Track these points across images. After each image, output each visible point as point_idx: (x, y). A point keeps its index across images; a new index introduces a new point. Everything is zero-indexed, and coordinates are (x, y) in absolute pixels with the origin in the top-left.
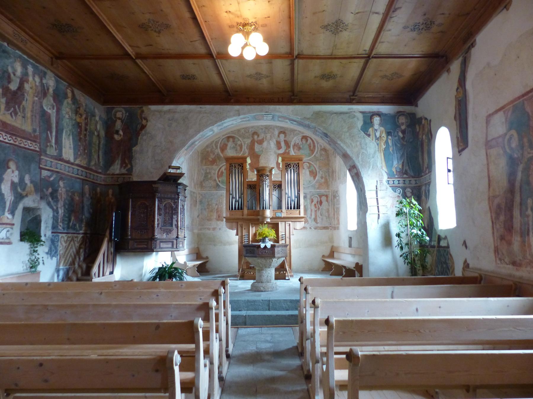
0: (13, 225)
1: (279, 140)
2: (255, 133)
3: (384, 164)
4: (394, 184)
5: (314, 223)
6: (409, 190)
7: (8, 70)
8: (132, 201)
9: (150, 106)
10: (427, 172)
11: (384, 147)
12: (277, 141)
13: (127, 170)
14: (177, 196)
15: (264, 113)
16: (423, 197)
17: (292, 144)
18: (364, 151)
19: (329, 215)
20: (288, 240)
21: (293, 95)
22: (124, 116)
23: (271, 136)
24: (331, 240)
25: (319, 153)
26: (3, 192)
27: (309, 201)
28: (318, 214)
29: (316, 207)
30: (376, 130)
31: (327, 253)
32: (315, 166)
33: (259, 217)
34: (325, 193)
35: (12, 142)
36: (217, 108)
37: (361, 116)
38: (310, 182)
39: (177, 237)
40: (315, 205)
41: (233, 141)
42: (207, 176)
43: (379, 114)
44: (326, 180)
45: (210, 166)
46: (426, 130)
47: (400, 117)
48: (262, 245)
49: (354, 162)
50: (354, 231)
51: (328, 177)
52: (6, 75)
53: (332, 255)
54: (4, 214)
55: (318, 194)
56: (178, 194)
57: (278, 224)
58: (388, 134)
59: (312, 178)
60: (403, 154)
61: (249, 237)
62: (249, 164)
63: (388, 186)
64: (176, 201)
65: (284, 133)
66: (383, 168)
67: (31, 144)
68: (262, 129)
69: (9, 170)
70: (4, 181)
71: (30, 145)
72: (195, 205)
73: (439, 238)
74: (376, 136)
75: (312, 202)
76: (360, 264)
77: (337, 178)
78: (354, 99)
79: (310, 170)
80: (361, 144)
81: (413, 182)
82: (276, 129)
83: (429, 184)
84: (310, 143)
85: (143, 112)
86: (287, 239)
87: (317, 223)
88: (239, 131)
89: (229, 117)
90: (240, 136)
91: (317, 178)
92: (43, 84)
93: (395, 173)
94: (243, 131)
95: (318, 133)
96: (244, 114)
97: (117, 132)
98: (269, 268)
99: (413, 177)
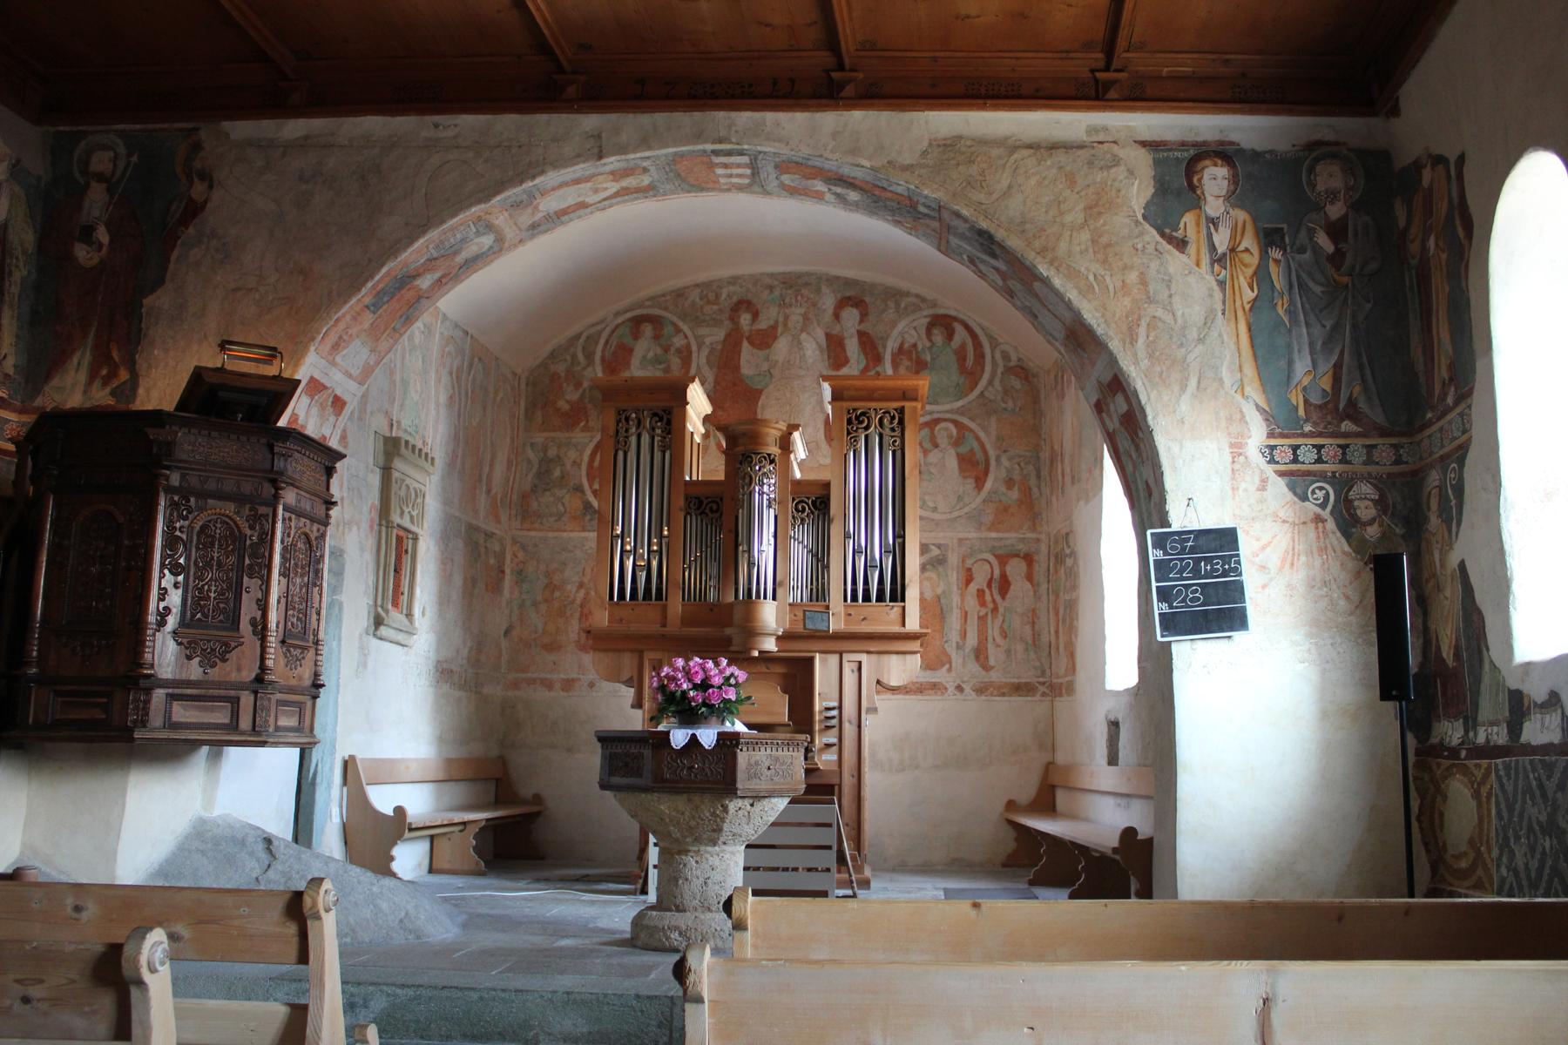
1: (836, 330)
2: (744, 304)
3: (1250, 370)
4: (1295, 460)
5: (973, 667)
6: (1363, 492)
8: (57, 506)
9: (226, 125)
10: (1450, 400)
11: (1249, 295)
12: (828, 336)
13: (113, 394)
14: (268, 490)
15: (709, 147)
16: (1434, 521)
17: (891, 346)
18: (1160, 313)
19: (1036, 636)
20: (849, 730)
21: (841, 68)
22: (121, 164)
23: (806, 318)
24: (1046, 737)
25: (997, 382)
27: (954, 577)
28: (993, 631)
29: (983, 604)
30: (1214, 222)
31: (1026, 793)
32: (982, 435)
33: (728, 631)
34: (1023, 548)
36: (506, 124)
37: (1143, 161)
38: (960, 498)
39: (259, 679)
40: (980, 593)
41: (657, 337)
42: (546, 475)
43: (1223, 153)
44: (1027, 492)
45: (561, 436)
46: (1441, 208)
47: (1318, 168)
48: (679, 738)
49: (1113, 361)
50: (1127, 690)
51: (1033, 482)
53: (1045, 802)
55: (993, 551)
56: (276, 481)
57: (811, 661)
58: (1270, 238)
59: (971, 481)
60: (1337, 327)
62: (706, 420)
63: (1269, 470)
64: (262, 510)
65: (859, 303)
66: (1248, 390)
68: (771, 288)
72: (495, 587)
73: (1519, 706)
74: (1212, 248)
75: (969, 579)
76: (1144, 832)
77: (1068, 479)
78: (1108, 85)
79: (963, 449)
80: (1143, 282)
81: (1384, 454)
82: (825, 289)
83: (1460, 453)
84: (963, 346)
85: (197, 147)
86: (846, 726)
87: (986, 667)
88: (680, 294)
89: (559, 163)
91: (988, 485)
93: (1301, 412)
94: (694, 295)
95: (954, 241)
96: (622, 150)
97: (87, 235)
98: (714, 843)
99: (1384, 433)
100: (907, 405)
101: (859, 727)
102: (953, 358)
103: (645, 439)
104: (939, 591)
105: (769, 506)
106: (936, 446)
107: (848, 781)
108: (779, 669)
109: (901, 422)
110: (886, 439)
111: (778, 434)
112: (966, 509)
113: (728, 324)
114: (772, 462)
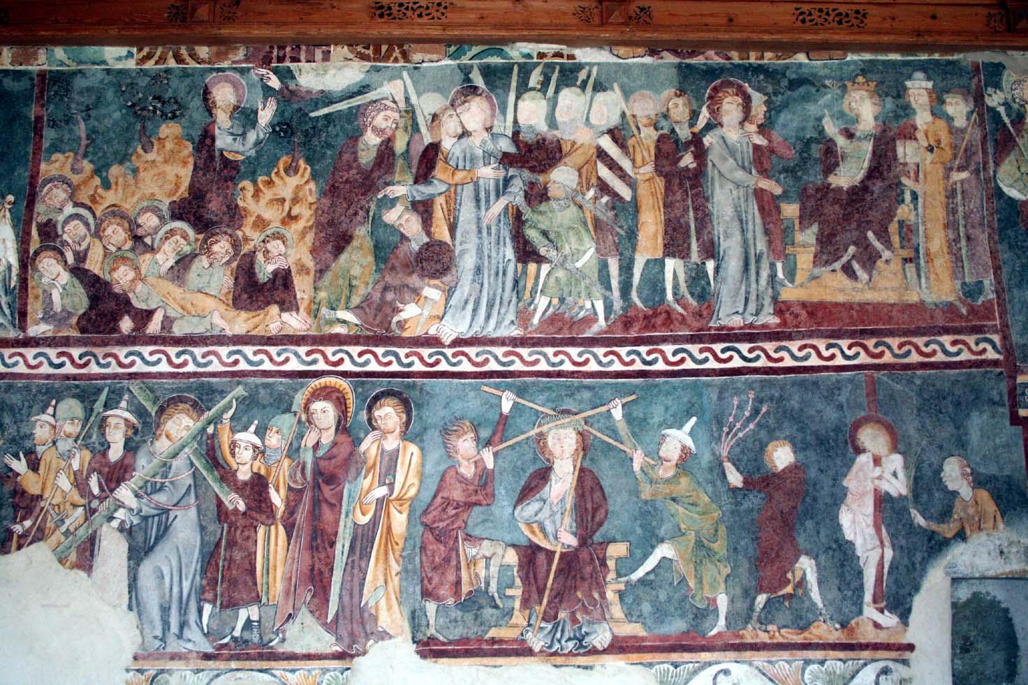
0: (911, 647)
7: (821, 132)
26: (849, 536)
35: (863, 359)
52: (816, 151)
54: (860, 612)
67: (954, 343)
69: (863, 459)
70: (849, 496)
71: (953, 349)
92: (992, 110)
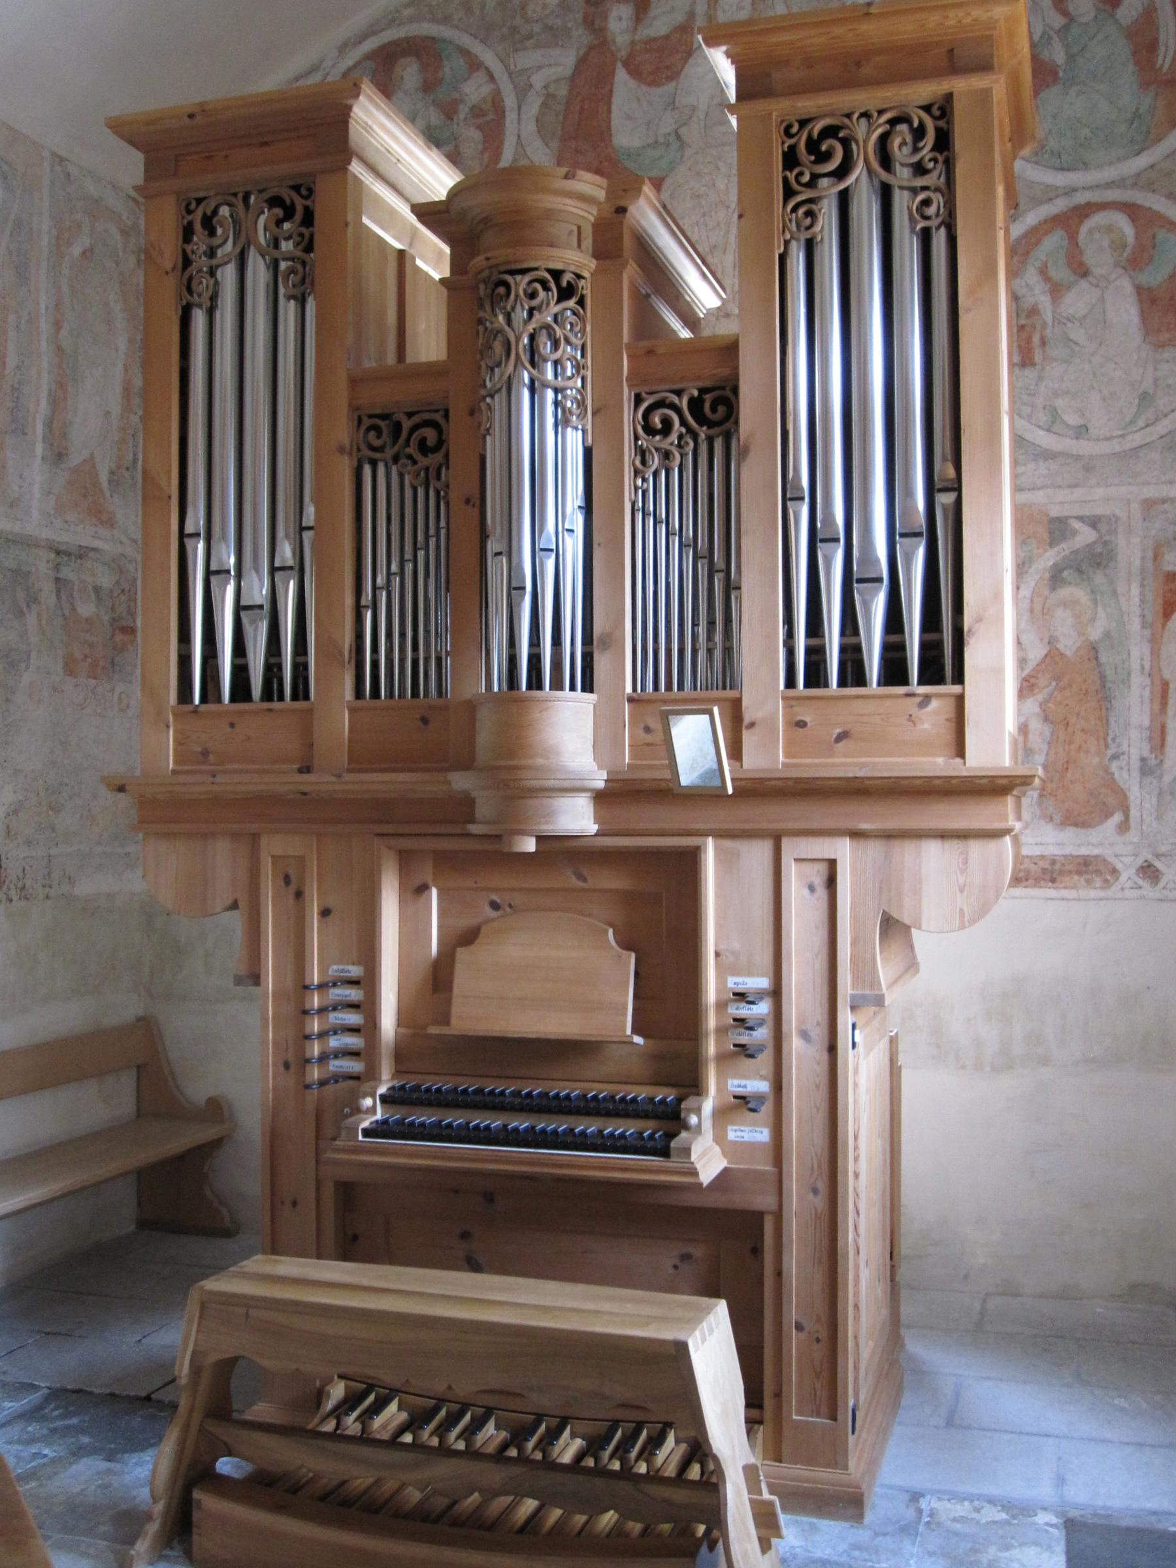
20: (802, 1054)
41: (428, 87)
57: (690, 860)
61: (369, 1007)
86: (795, 1045)
90: (485, 33)
100: (959, 85)
101: (832, 1049)
102: (1123, 48)
103: (258, 272)
104: (1095, 633)
105: (562, 423)
106: (1083, 272)
107: (799, 1202)
108: (613, 881)
109: (943, 142)
110: (902, 202)
111: (588, 215)
112: (1163, 427)
113: (581, 37)
114: (566, 293)
